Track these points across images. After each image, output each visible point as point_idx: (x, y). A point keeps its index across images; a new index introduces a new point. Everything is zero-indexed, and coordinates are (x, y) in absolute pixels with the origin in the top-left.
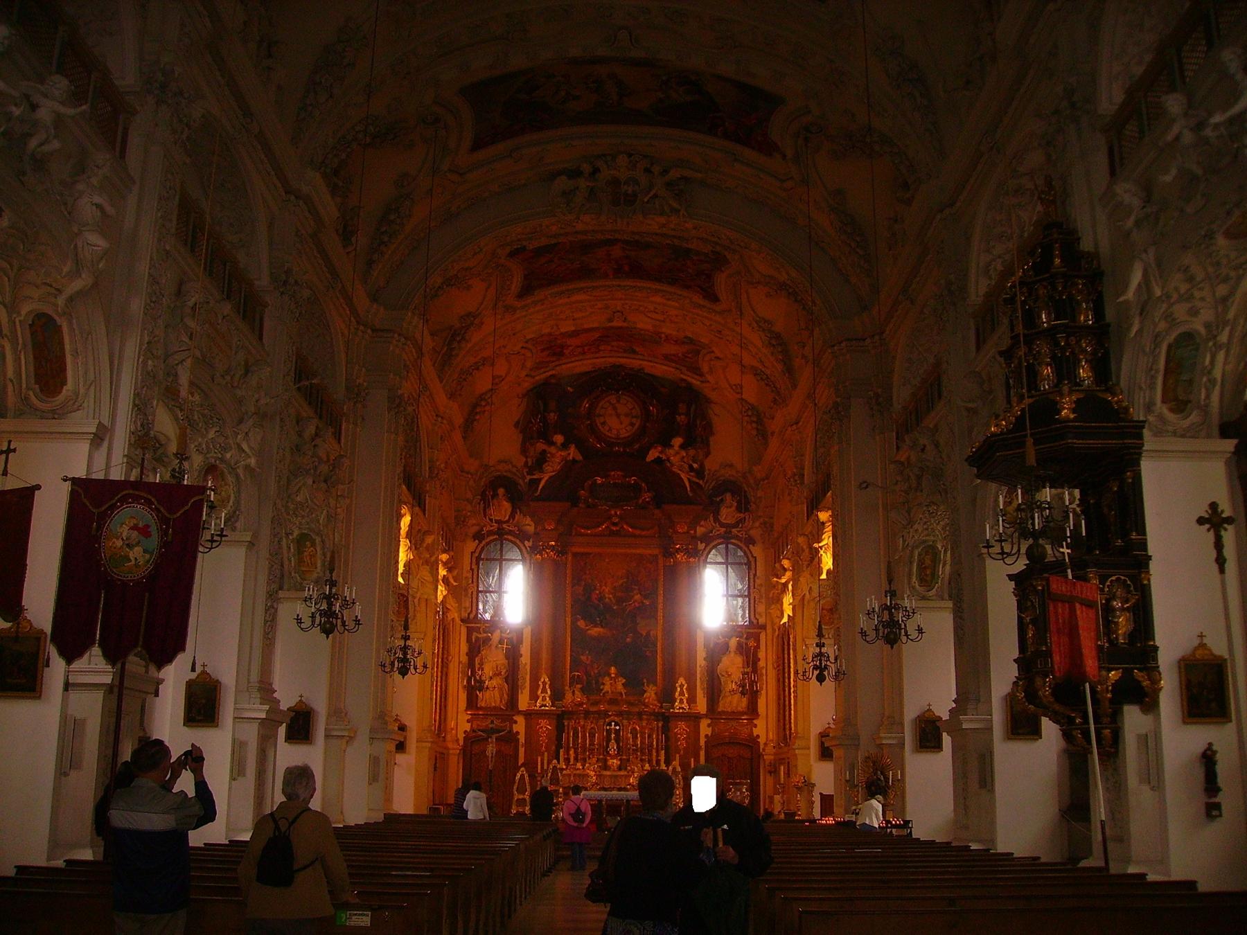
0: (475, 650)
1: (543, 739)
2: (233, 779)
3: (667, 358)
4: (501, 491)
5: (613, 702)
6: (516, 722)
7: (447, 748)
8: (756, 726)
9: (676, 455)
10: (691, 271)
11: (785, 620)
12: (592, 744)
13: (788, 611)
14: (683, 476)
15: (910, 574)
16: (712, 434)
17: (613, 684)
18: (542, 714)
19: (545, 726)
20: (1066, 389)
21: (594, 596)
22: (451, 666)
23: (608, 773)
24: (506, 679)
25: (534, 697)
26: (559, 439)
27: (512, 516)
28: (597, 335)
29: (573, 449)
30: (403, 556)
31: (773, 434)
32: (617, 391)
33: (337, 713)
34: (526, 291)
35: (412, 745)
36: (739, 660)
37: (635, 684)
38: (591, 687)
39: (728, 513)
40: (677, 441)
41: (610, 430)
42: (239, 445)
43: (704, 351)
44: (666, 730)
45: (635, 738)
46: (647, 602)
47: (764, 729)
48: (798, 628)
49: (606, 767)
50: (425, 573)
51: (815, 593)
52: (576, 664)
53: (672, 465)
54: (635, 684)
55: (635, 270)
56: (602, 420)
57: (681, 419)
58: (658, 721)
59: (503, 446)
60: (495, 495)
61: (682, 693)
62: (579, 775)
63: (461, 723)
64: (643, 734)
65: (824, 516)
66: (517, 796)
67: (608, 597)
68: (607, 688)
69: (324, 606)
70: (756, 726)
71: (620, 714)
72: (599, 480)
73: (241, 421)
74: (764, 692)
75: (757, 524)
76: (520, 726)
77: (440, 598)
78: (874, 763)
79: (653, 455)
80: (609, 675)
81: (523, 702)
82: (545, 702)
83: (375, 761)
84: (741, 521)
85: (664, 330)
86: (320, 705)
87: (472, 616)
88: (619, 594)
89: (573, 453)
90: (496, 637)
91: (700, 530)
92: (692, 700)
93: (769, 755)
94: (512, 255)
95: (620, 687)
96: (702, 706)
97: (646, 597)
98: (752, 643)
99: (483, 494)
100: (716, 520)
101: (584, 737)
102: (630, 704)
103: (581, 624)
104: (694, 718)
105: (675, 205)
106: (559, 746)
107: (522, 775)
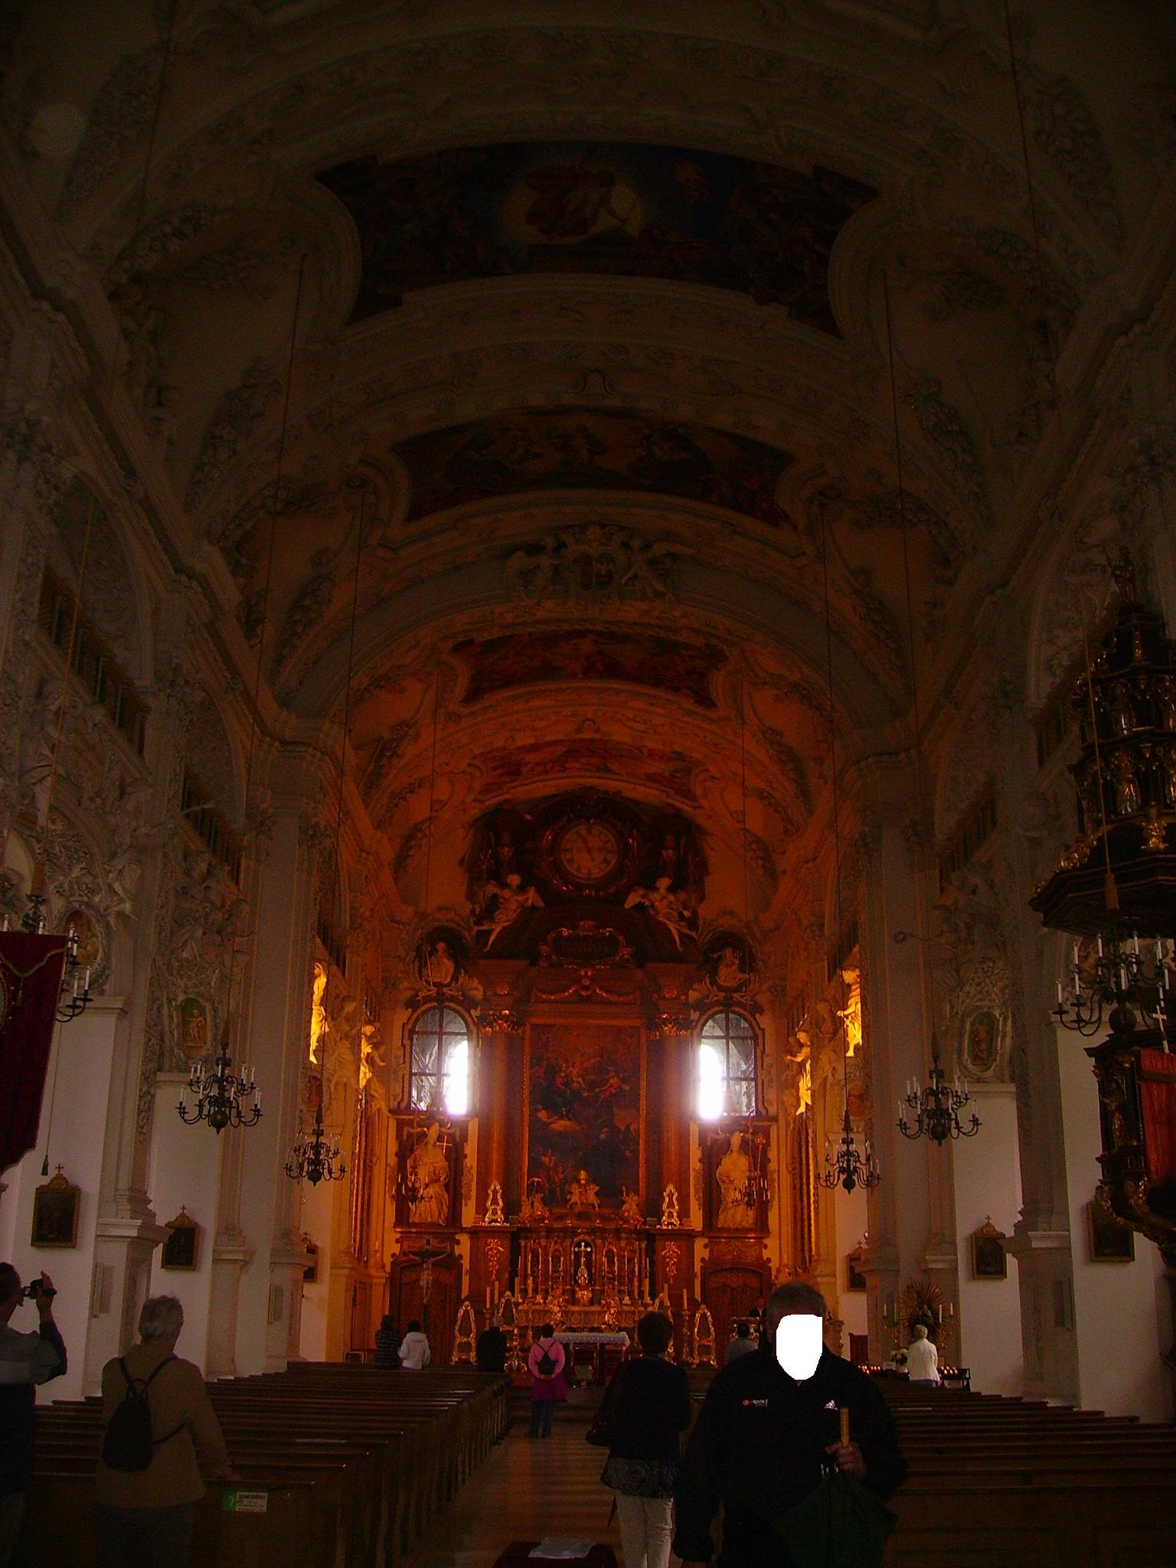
0: (408, 1148)
1: (493, 1265)
2: (93, 1315)
3: (650, 778)
4: (441, 946)
6: (458, 1242)
7: (371, 1277)
8: (766, 1247)
9: (662, 900)
10: (680, 669)
11: (802, 1109)
13: (806, 1098)
14: (671, 926)
15: (960, 1051)
16: (708, 873)
17: (583, 1194)
18: (492, 1232)
19: (496, 1248)
20: (1153, 812)
21: (559, 1080)
22: (376, 1169)
23: (577, 1308)
24: (446, 1186)
25: (481, 1210)
26: (515, 880)
27: (455, 978)
28: (561, 749)
29: (532, 891)
30: (316, 1028)
31: (784, 872)
32: (588, 819)
33: (229, 1229)
34: (473, 695)
35: (325, 1271)
36: (743, 1162)
37: (611, 1195)
38: (555, 1198)
39: (728, 975)
40: (664, 883)
42: (110, 887)
44: (651, 1252)
45: (611, 1263)
46: (627, 1088)
47: (776, 1251)
48: (819, 1120)
49: (574, 1301)
50: (344, 1050)
51: (840, 1075)
52: (536, 1166)
53: (658, 913)
54: (611, 1195)
55: (612, 670)
57: (668, 854)
58: (640, 1241)
59: (445, 889)
60: (434, 951)
61: (671, 1205)
62: (539, 1312)
63: (388, 1244)
65: (849, 976)
66: (460, 1339)
67: (578, 1082)
68: (575, 1198)
69: (215, 1092)
71: (592, 1231)
72: (565, 932)
73: (114, 856)
74: (775, 1202)
75: (765, 987)
76: (464, 1247)
77: (363, 1083)
78: (918, 1293)
79: (633, 899)
80: (578, 1181)
81: (468, 1216)
82: (495, 1216)
83: (276, 1292)
85: (645, 743)
86: (207, 1220)
87: (403, 1105)
89: (532, 897)
90: (433, 1132)
91: (693, 996)
92: (684, 1213)
94: (457, 649)
95: (592, 1198)
97: (624, 1080)
98: (760, 1140)
100: (713, 982)
101: (546, 1262)
102: (605, 1219)
103: (543, 1115)
104: (686, 1237)
105: (661, 588)
106: (513, 1274)
107: (466, 1311)
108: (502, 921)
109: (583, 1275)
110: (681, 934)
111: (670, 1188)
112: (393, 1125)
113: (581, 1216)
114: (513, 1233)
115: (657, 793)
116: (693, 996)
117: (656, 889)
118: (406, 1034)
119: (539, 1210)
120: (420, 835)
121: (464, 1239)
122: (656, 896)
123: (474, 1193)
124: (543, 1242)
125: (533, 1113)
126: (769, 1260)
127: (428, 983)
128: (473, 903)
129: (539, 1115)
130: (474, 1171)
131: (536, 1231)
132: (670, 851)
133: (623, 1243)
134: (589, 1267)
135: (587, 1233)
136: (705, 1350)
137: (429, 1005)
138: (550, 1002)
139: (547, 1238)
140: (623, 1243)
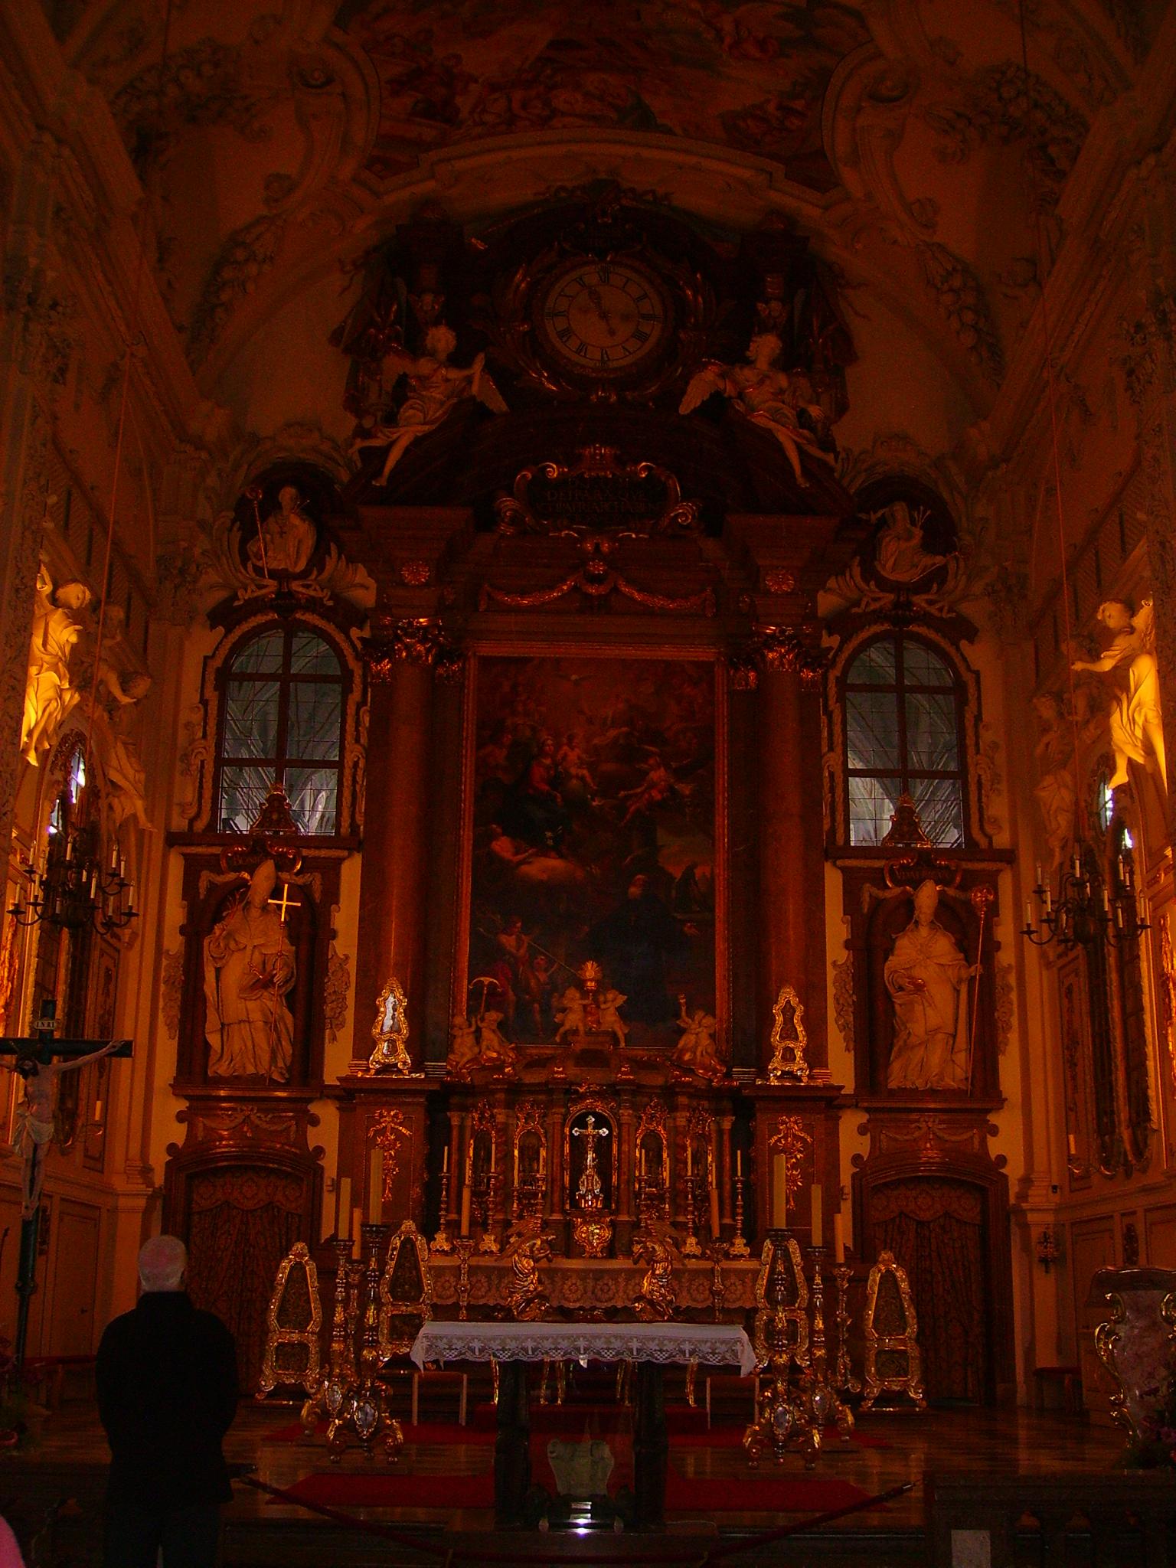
0: (206, 913)
4: (287, 495)
5: (591, 1058)
6: (315, 1121)
8: (994, 1131)
9: (763, 389)
12: (528, 1179)
14: (785, 437)
19: (395, 1125)
24: (290, 1000)
27: (317, 560)
36: (943, 946)
37: (654, 1012)
38: (526, 1018)
39: (901, 555)
40: (765, 347)
41: (582, 348)
46: (685, 789)
49: (569, 1246)
52: (486, 955)
53: (751, 409)
54: (654, 1012)
58: (719, 1113)
59: (296, 388)
60: (270, 506)
62: (488, 1271)
64: (678, 1150)
66: (280, 1336)
68: (573, 1020)
70: (994, 1131)
71: (611, 1092)
72: (553, 471)
74: (1013, 1037)
76: (326, 1129)
80: (580, 985)
81: (338, 1061)
84: (939, 575)
87: (200, 826)
92: (816, 1056)
93: (1041, 1211)
95: (610, 1019)
96: (841, 1069)
98: (978, 897)
99: (242, 507)
100: (870, 573)
101: (506, 1158)
102: (639, 1065)
103: (503, 846)
104: (825, 1104)
107: (298, 1268)
109: (590, 1187)
110: (801, 452)
111: (788, 995)
113: (591, 1058)
114: (431, 1096)
115: (747, 174)
116: (827, 602)
117: (749, 363)
118: (211, 677)
119: (493, 1047)
120: (240, 255)
121: (328, 1113)
122: (746, 375)
123: (350, 1015)
125: (482, 841)
126: (1002, 1160)
127: (259, 571)
128: (359, 414)
130: (352, 968)
133: (682, 1122)
135: (600, 1095)
136: (893, 1363)
137: (261, 619)
138: (520, 610)
139: (509, 1105)
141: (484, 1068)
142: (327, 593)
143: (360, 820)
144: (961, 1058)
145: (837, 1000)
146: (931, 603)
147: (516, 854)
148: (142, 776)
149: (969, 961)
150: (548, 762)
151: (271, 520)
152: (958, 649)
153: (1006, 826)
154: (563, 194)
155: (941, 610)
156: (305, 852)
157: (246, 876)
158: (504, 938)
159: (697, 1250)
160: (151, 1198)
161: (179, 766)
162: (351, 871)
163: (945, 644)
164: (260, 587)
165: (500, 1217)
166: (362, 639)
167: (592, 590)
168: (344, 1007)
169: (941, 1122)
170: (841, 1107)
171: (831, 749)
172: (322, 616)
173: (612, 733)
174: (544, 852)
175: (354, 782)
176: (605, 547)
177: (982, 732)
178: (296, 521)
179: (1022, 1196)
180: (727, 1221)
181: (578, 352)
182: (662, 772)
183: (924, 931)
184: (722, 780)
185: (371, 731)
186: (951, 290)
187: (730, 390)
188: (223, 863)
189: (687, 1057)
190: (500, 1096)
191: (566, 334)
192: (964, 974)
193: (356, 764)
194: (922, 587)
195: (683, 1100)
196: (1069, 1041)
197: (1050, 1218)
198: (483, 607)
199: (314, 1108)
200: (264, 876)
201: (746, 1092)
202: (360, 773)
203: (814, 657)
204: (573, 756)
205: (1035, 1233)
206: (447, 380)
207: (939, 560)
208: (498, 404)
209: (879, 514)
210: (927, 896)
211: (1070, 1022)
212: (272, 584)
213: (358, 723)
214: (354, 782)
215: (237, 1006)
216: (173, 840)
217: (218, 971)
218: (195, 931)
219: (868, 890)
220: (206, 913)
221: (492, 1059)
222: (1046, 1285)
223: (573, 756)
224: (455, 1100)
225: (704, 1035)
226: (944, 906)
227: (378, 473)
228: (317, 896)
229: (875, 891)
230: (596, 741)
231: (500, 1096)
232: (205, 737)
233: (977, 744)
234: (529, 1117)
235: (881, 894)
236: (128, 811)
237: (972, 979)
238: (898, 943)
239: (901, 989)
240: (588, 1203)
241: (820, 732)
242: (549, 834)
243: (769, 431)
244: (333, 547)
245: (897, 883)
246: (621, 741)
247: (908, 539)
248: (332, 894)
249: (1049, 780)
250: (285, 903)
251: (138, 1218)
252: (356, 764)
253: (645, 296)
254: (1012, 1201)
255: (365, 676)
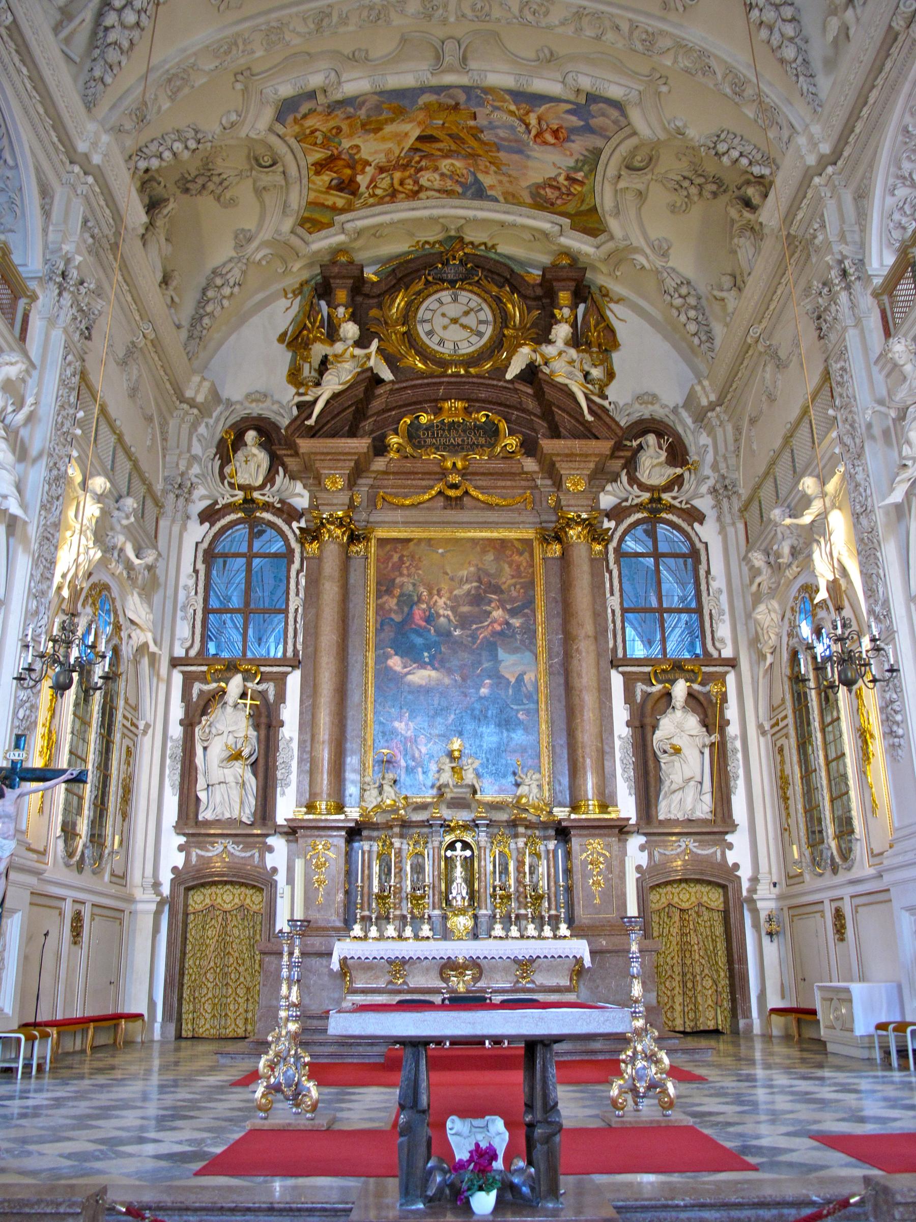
0: (197, 711)
3: (541, 200)
4: (251, 436)
6: (270, 849)
7: (131, 899)
8: (730, 846)
9: (561, 360)
27: (270, 478)
36: (692, 722)
39: (653, 466)
40: (562, 331)
41: (441, 342)
43: (603, 158)
53: (552, 372)
56: (427, 327)
58: (546, 838)
60: (239, 442)
64: (520, 863)
70: (730, 846)
71: (471, 826)
75: (704, 489)
81: (286, 808)
84: (678, 481)
87: (193, 653)
88: (465, 609)
96: (626, 806)
97: (513, 613)
100: (633, 480)
101: (401, 870)
103: (395, 663)
108: (334, 382)
110: (587, 398)
112: (177, 678)
113: (458, 804)
116: (607, 501)
120: (219, 281)
122: (550, 350)
123: (294, 777)
124: (397, 843)
125: (381, 659)
126: (736, 866)
127: (232, 485)
129: (390, 662)
130: (295, 745)
131: (389, 826)
132: (566, 312)
134: (469, 881)
135: (465, 827)
137: (233, 517)
138: (403, 507)
139: (402, 836)
140: (521, 842)
141: (384, 811)
142: (277, 498)
143: (299, 647)
144: (707, 798)
145: (622, 761)
146: (674, 498)
147: (405, 667)
148: (151, 617)
149: (709, 732)
150: (424, 606)
151: (239, 453)
152: (693, 529)
153: (729, 642)
154: (427, 246)
155: (681, 502)
156: (263, 669)
157: (223, 684)
158: (396, 724)
159: (536, 934)
160: (160, 904)
161: (180, 614)
162: (294, 680)
163: (684, 525)
164: (232, 496)
165: (398, 912)
166: (300, 529)
167: (451, 493)
168: (289, 773)
169: (695, 841)
170: (628, 833)
171: (612, 594)
172: (274, 514)
173: (467, 587)
174: (423, 666)
175: (295, 621)
176: (459, 465)
177: (711, 582)
178: (255, 450)
179: (753, 890)
180: (553, 912)
181: (439, 344)
182: (500, 612)
183: (679, 713)
184: (540, 617)
185: (307, 588)
186: (680, 296)
187: (539, 360)
188: (209, 677)
189: (524, 801)
190: (397, 830)
191: (430, 333)
192: (707, 741)
193: (296, 610)
194: (668, 488)
195: (521, 830)
196: (783, 783)
197: (772, 905)
198: (380, 504)
199: (270, 841)
200: (236, 684)
201: (564, 824)
202: (299, 617)
203: (597, 535)
204: (441, 602)
205: (763, 915)
206: (354, 356)
207: (679, 471)
208: (387, 375)
209: (638, 442)
210: (680, 689)
211: (782, 771)
212: (240, 495)
213: (297, 584)
214: (295, 621)
215: (216, 774)
216: (175, 663)
217: (205, 749)
218: (189, 724)
219: (640, 687)
220: (197, 711)
221: (388, 806)
222: (771, 949)
223: (441, 602)
224: (365, 833)
225: (534, 786)
226: (691, 695)
227: (309, 416)
228: (271, 698)
229: (644, 687)
230: (455, 592)
231: (397, 830)
232: (196, 593)
233: (708, 590)
234: (416, 843)
235: (650, 690)
236: (142, 640)
237: (712, 745)
238: (662, 722)
239: (665, 752)
240: (458, 903)
241: (604, 583)
242: (426, 654)
243: (566, 385)
244: (281, 470)
245: (659, 682)
246: (473, 592)
247: (658, 458)
248: (281, 697)
249: (762, 608)
250: (249, 702)
251: (151, 918)
252: (296, 610)
253: (482, 309)
254: (745, 893)
255: (302, 553)
